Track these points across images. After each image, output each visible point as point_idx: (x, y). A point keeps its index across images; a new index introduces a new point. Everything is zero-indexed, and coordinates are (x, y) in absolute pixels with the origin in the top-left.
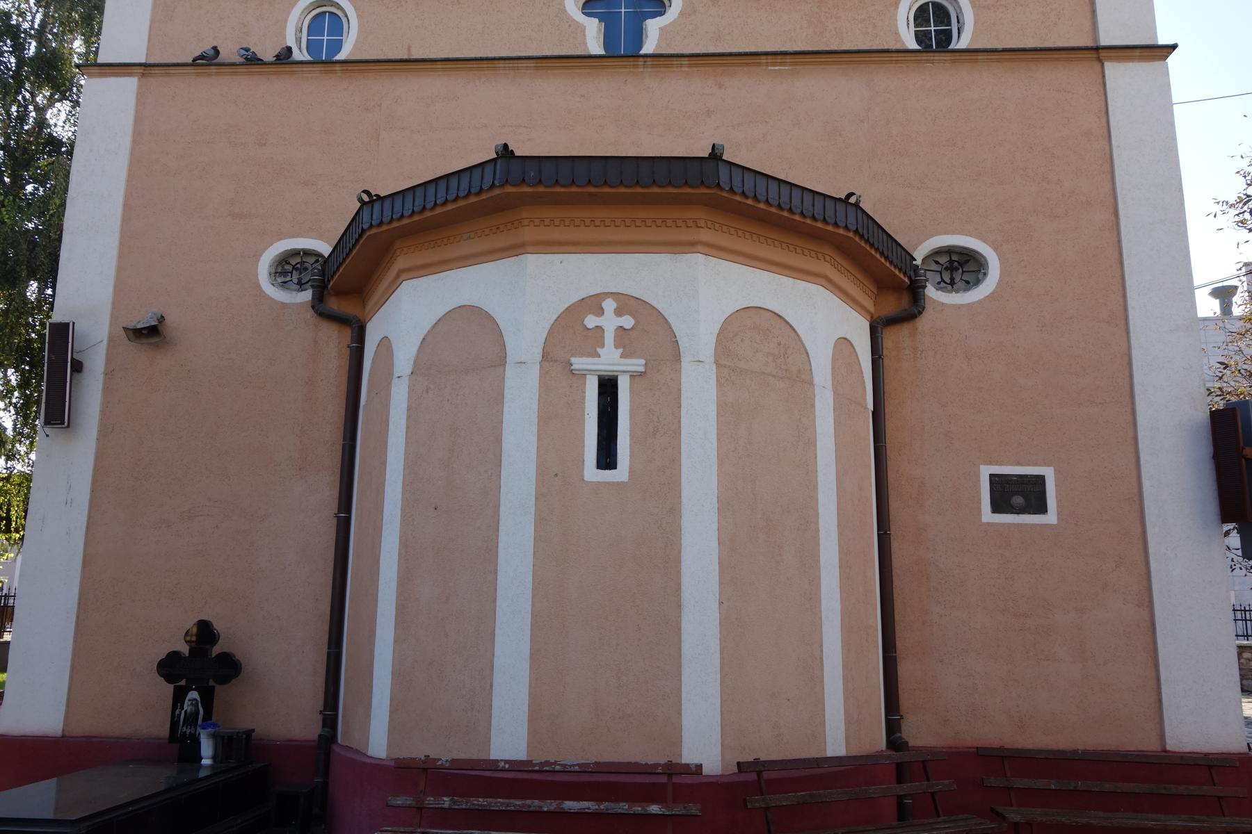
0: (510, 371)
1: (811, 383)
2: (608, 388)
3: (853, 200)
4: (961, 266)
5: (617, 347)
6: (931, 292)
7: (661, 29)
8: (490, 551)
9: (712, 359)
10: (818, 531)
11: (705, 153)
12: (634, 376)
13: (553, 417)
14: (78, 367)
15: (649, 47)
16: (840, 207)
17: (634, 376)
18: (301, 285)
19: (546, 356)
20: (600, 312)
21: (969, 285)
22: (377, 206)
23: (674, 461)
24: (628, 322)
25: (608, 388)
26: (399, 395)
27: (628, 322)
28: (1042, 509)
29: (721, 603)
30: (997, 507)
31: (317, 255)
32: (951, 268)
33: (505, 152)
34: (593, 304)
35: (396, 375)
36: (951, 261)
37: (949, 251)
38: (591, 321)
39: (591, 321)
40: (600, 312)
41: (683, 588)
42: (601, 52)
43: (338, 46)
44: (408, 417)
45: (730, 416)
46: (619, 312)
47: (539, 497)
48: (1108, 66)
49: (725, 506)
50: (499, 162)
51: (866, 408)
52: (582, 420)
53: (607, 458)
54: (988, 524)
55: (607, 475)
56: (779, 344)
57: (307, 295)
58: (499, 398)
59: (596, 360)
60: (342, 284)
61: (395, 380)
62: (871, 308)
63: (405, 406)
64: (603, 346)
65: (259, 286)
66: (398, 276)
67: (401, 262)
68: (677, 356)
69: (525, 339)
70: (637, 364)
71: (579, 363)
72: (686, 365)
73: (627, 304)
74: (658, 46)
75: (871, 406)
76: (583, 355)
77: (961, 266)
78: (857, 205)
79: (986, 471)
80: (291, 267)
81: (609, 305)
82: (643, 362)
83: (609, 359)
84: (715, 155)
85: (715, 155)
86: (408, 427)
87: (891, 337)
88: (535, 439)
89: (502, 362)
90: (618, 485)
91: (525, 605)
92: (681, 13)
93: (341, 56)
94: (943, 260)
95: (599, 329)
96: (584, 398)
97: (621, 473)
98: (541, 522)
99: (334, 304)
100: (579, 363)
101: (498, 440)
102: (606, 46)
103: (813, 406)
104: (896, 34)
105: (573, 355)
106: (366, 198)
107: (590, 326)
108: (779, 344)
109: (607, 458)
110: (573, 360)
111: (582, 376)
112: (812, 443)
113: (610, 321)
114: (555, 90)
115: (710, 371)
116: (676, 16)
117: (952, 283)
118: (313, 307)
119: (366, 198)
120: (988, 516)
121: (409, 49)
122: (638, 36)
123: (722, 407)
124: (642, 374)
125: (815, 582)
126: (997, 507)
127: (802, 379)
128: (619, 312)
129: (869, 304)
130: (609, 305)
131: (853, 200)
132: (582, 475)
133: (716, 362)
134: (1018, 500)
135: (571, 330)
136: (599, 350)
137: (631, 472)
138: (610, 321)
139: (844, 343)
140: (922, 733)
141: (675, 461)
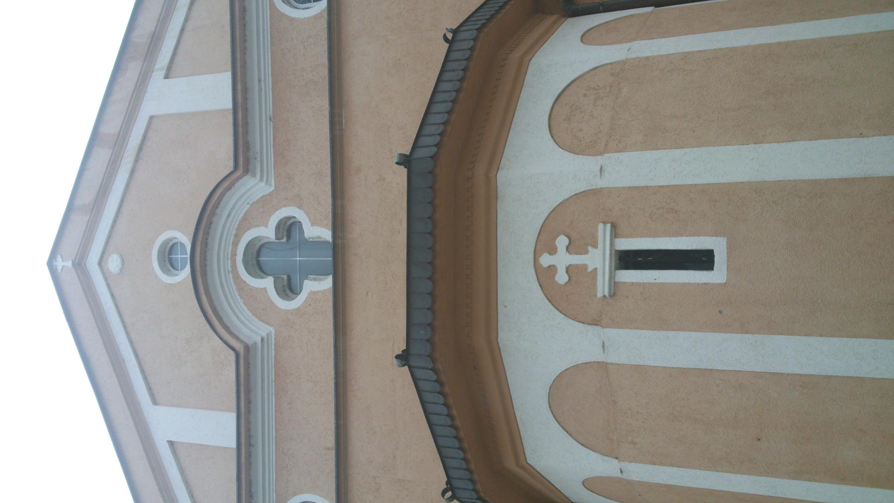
0: (613, 358)
1: (624, 62)
3: (450, 36)
5: (587, 252)
7: (313, 224)
8: (807, 384)
9: (599, 158)
10: (779, 44)
11: (403, 171)
13: (659, 315)
15: (326, 234)
16: (457, 46)
19: (595, 323)
20: (552, 269)
22: (456, 483)
23: (706, 191)
24: (562, 242)
26: (640, 472)
27: (562, 242)
29: (861, 135)
33: (404, 358)
34: (544, 276)
35: (619, 475)
38: (562, 278)
39: (562, 278)
40: (552, 269)
41: (845, 176)
42: (330, 279)
44: (661, 464)
45: (656, 137)
46: (553, 251)
47: (744, 329)
49: (752, 134)
50: (413, 363)
51: (652, 13)
52: (663, 285)
53: (702, 260)
55: (720, 259)
56: (585, 95)
58: (639, 370)
59: (600, 272)
61: (625, 476)
62: (555, 17)
63: (650, 467)
64: (585, 266)
66: (522, 467)
67: (511, 464)
68: (595, 193)
70: (603, 232)
73: (544, 243)
74: (325, 226)
75: (652, 8)
78: (455, 32)
81: (546, 260)
82: (601, 226)
83: (598, 259)
84: (405, 161)
85: (405, 161)
86: (672, 465)
88: (682, 334)
89: (602, 366)
90: (731, 248)
91: (868, 345)
92: (300, 207)
95: (568, 270)
96: (638, 284)
97: (717, 245)
98: (771, 328)
100: (602, 288)
101: (684, 372)
102: (328, 274)
103: (647, 58)
104: (315, 17)
105: (595, 296)
106: (449, 494)
107: (566, 278)
108: (585, 95)
109: (702, 260)
110: (600, 295)
111: (615, 286)
112: (686, 56)
115: (609, 160)
116: (302, 212)
119: (449, 494)
121: (328, 449)
122: (317, 244)
123: (648, 144)
124: (614, 226)
125: (835, 42)
127: (618, 72)
128: (553, 251)
130: (546, 260)
131: (450, 36)
132: (720, 285)
133: (601, 154)
135: (569, 298)
136: (590, 269)
137: (716, 234)
138: (561, 260)
139: (585, 38)
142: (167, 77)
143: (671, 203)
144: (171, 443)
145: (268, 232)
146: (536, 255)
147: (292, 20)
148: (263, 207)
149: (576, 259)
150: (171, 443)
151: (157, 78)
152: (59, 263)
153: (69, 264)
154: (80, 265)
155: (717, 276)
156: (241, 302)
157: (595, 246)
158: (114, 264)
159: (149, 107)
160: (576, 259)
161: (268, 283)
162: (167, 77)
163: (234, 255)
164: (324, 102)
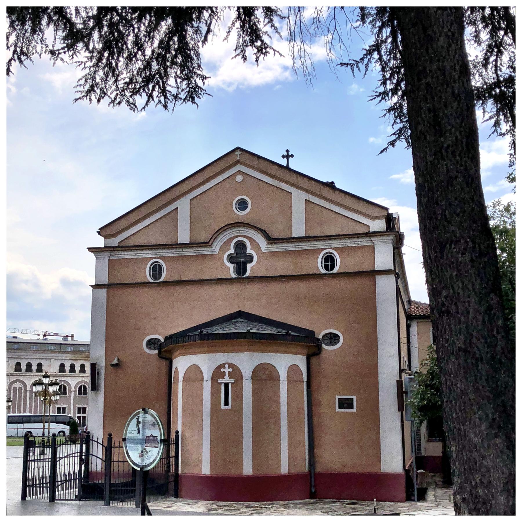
0: (205, 382)
2: (226, 385)
4: (333, 339)
6: (324, 346)
12: (232, 383)
13: (215, 393)
14: (98, 373)
17: (232, 383)
18: (155, 349)
20: (224, 368)
21: (336, 343)
24: (231, 370)
25: (226, 385)
27: (231, 370)
28: (352, 408)
30: (340, 407)
31: (159, 340)
32: (331, 338)
34: (223, 366)
36: (331, 337)
37: (330, 333)
38: (222, 370)
39: (222, 370)
40: (224, 368)
43: (160, 275)
45: (254, 391)
46: (229, 368)
48: (376, 276)
53: (226, 403)
54: (338, 412)
55: (227, 407)
57: (156, 352)
60: (166, 349)
65: (143, 349)
68: (242, 378)
69: (207, 375)
70: (233, 381)
71: (220, 381)
72: (244, 380)
73: (231, 365)
76: (220, 378)
77: (333, 339)
79: (337, 397)
80: (151, 343)
81: (227, 366)
83: (227, 379)
87: (314, 360)
89: (203, 380)
90: (229, 409)
93: (161, 280)
94: (329, 336)
95: (224, 372)
97: (229, 407)
99: (164, 354)
100: (220, 381)
109: (226, 403)
111: (221, 383)
113: (227, 370)
114: (221, 290)
117: (331, 343)
118: (159, 355)
120: (337, 409)
124: (234, 383)
126: (340, 407)
128: (229, 368)
129: (305, 351)
130: (227, 366)
134: (345, 405)
138: (227, 370)
140: (319, 469)
141: (242, 403)
142: (306, 200)
143: (238, 396)
144: (177, 208)
145: (249, 250)
146: (228, 363)
147: (318, 257)
148: (258, 246)
149: (227, 374)
150: (177, 208)
151: (305, 196)
152: (238, 153)
153: (238, 159)
154: (238, 162)
155: (223, 407)
156: (225, 240)
157: (230, 378)
158: (239, 178)
159: (295, 192)
160: (227, 374)
161: (232, 251)
162: (306, 200)
163: (241, 236)
164: (290, 273)
